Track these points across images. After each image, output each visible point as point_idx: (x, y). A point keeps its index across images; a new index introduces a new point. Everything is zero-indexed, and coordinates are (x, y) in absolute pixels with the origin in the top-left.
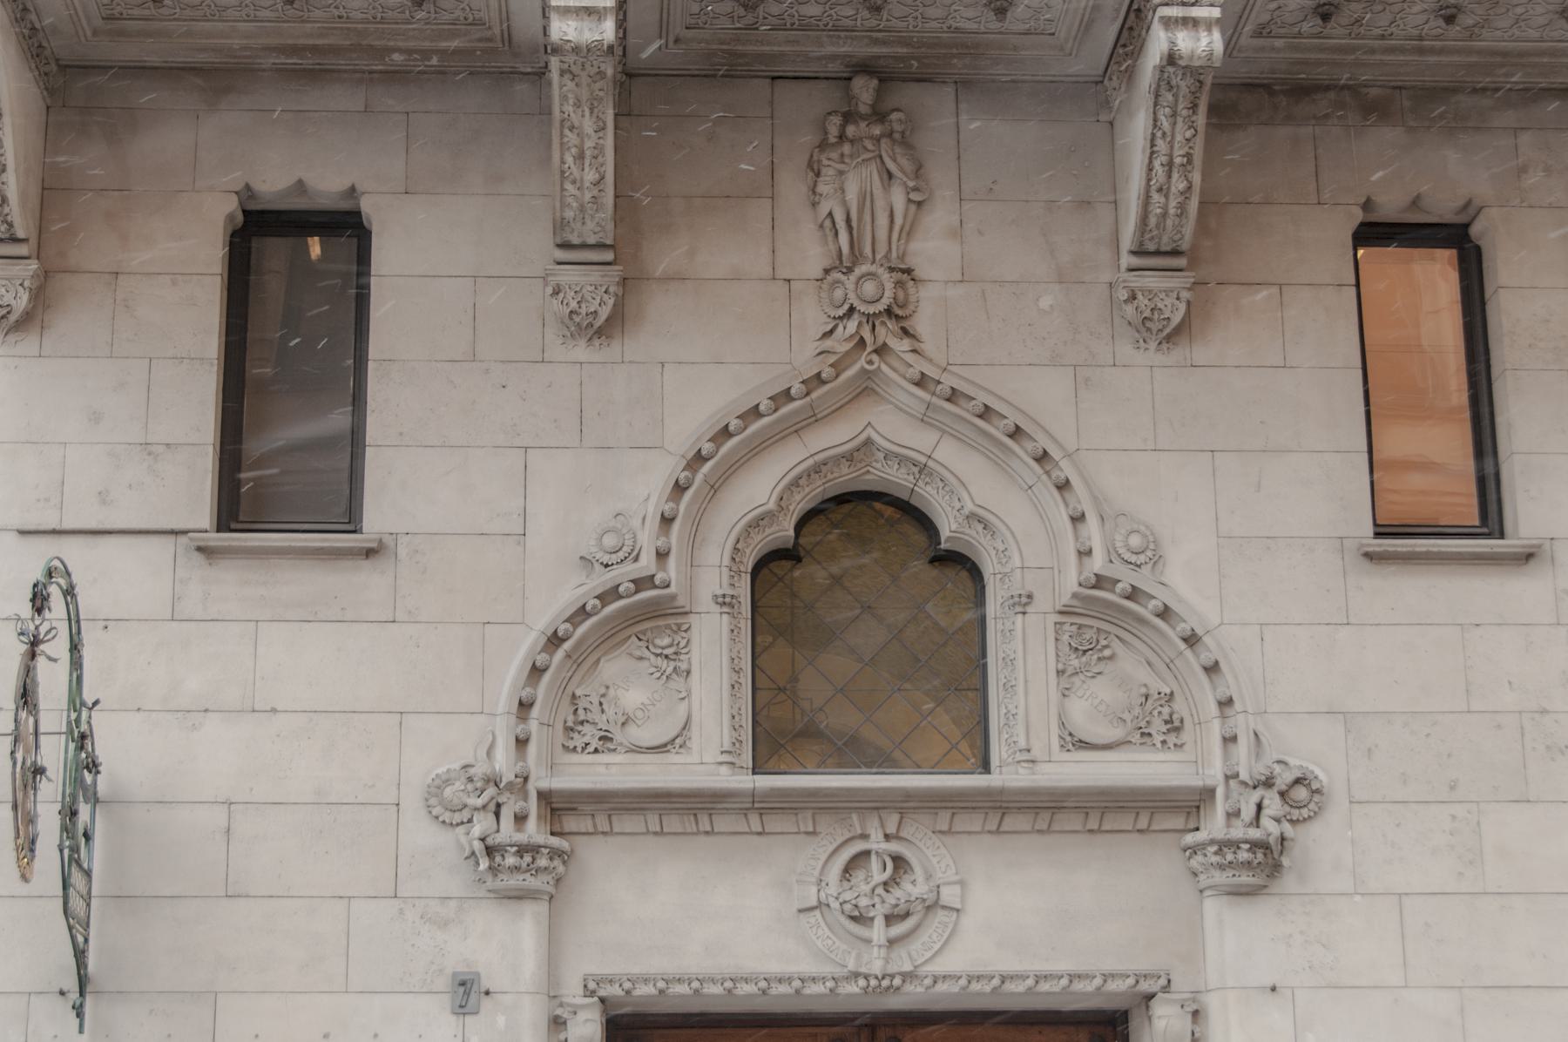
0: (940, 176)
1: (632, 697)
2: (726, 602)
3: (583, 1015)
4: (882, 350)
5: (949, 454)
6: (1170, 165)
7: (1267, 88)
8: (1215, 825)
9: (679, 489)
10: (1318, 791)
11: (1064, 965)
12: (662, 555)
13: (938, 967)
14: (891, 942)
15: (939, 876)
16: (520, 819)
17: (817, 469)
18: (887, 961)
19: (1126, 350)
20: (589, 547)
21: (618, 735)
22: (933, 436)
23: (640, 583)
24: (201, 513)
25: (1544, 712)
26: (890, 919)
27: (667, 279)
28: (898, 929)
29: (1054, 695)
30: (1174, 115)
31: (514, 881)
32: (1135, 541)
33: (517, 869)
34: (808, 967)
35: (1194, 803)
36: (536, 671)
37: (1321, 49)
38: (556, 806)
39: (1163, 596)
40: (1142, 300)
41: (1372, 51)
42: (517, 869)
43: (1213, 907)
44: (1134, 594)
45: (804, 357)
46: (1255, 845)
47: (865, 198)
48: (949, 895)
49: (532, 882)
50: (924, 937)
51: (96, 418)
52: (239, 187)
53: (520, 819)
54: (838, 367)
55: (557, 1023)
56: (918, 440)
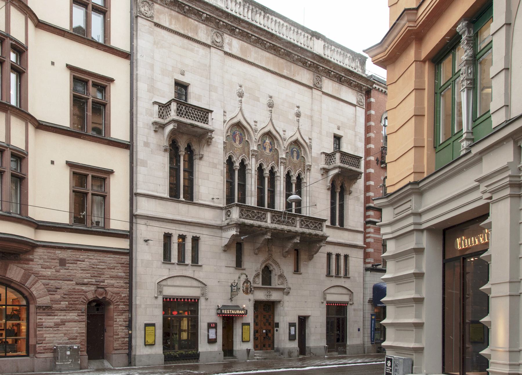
5: (273, 264)
8: (285, 291)
24: (235, 266)
34: (265, 299)
35: (284, 289)
43: (285, 296)
56: (271, 263)
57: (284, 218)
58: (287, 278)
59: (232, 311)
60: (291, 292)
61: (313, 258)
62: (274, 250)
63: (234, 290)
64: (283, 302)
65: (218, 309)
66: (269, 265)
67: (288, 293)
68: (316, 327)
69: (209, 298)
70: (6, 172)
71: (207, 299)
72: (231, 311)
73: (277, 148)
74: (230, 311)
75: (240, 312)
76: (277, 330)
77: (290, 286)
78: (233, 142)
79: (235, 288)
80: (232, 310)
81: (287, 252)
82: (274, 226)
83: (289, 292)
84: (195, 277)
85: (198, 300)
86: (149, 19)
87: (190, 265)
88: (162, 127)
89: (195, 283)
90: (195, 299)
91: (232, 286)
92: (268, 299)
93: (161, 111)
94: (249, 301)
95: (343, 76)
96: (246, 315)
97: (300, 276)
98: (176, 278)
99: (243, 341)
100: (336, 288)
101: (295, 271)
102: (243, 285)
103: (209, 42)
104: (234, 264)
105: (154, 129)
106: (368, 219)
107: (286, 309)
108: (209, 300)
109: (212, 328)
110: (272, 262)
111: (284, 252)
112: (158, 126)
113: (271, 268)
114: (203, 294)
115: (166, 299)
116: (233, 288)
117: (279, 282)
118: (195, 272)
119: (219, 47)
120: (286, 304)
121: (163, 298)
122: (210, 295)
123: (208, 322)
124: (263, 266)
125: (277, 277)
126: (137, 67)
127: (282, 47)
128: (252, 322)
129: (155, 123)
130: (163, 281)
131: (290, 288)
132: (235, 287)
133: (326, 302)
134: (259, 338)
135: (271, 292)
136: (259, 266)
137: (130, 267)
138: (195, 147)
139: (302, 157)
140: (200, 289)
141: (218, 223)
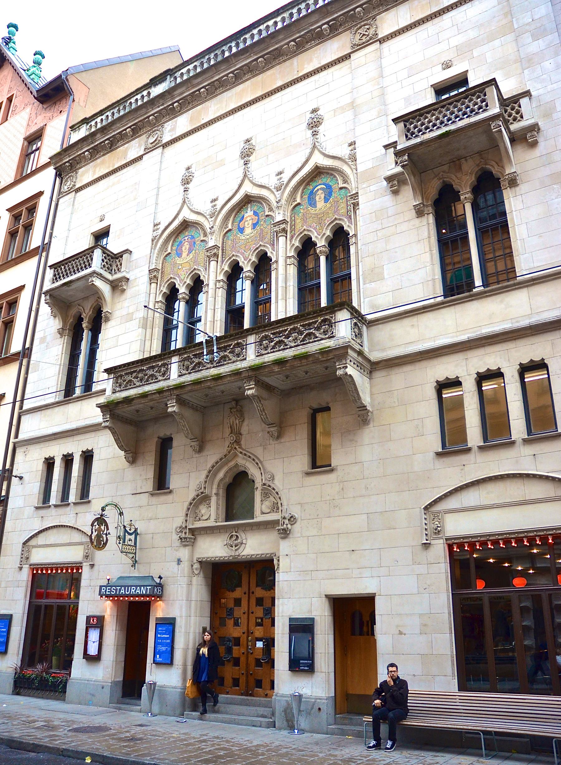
0: (246, 416)
1: (203, 512)
2: (217, 494)
3: (195, 564)
4: (235, 448)
6: (261, 411)
7: (295, 388)
9: (207, 476)
10: (295, 519)
11: (260, 552)
12: (205, 488)
13: (242, 554)
14: (236, 550)
15: (243, 538)
16: (185, 533)
17: (230, 469)
18: (235, 553)
19: (271, 441)
20: (196, 488)
21: (201, 518)
22: (245, 461)
23: (202, 493)
25: (334, 499)
26: (236, 546)
27: (208, 441)
28: (236, 548)
29: (260, 505)
30: (258, 403)
31: (184, 543)
32: (269, 476)
33: (184, 541)
34: (225, 555)
35: (276, 522)
36: (188, 509)
37: (295, 381)
38: (192, 531)
39: (272, 485)
40: (271, 433)
41: (304, 380)
42: (184, 541)
43: (280, 540)
44: (269, 486)
45: (225, 450)
46: (283, 529)
47: (233, 422)
48: (244, 541)
49: (187, 543)
50: (240, 549)
51: (141, 475)
52: (157, 436)
53: (185, 533)
54: (229, 452)
55: (192, 566)
60: (296, 528)
63: (130, 543)
68: (401, 633)
69: (95, 564)
71: (92, 566)
73: (270, 213)
77: (296, 511)
78: (177, 258)
94: (178, 564)
97: (331, 477)
98: (50, 532)
104: (149, 486)
108: (96, 567)
109: (95, 627)
114: (87, 557)
128: (181, 617)
131: (292, 519)
134: (243, 659)
135: (242, 535)
140: (83, 546)
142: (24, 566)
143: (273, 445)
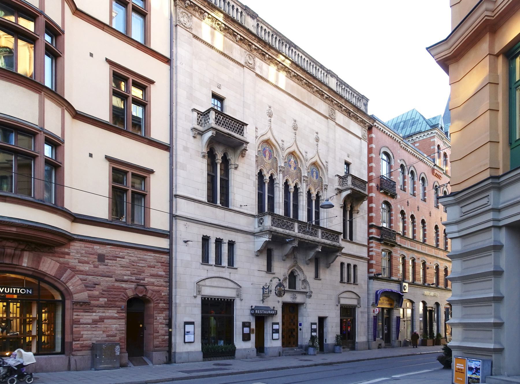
5: (298, 270)
8: (308, 294)
43: (307, 299)
56: (296, 269)
57: (309, 228)
58: (309, 283)
59: (264, 312)
61: (330, 266)
62: (298, 257)
63: (266, 292)
64: (306, 304)
65: (252, 309)
66: (294, 271)
67: (310, 296)
70: (39, 157)
71: (242, 300)
72: (263, 311)
74: (262, 312)
75: (271, 312)
76: (300, 329)
77: (312, 290)
79: (267, 290)
80: (264, 310)
81: (309, 260)
82: (300, 235)
83: (311, 296)
84: (231, 279)
85: (234, 300)
86: (188, 30)
87: (226, 267)
88: (201, 133)
89: (231, 285)
90: (231, 300)
91: (263, 288)
92: (294, 301)
93: (200, 119)
94: (278, 303)
95: (352, 112)
96: (276, 315)
99: (273, 339)
100: (348, 293)
101: (315, 277)
102: (276, 288)
103: (243, 63)
104: (265, 269)
105: (193, 135)
106: (371, 236)
107: (309, 310)
108: (243, 301)
110: (297, 268)
111: (307, 259)
112: (196, 133)
113: (296, 274)
114: (238, 295)
115: (205, 298)
116: (265, 290)
117: (303, 287)
118: (231, 274)
119: (252, 69)
120: (309, 306)
121: (202, 298)
122: (244, 296)
123: (243, 321)
124: (290, 272)
125: (301, 282)
126: (176, 73)
127: (304, 78)
129: (194, 129)
130: (202, 281)
132: (266, 289)
133: (339, 305)
135: (296, 294)
136: (286, 271)
137: (169, 266)
138: (231, 157)
139: (320, 177)
141: (251, 229)
142: (198, 296)
143: (306, 266)
